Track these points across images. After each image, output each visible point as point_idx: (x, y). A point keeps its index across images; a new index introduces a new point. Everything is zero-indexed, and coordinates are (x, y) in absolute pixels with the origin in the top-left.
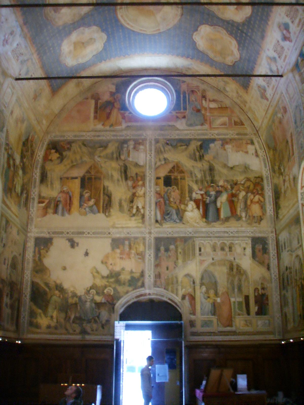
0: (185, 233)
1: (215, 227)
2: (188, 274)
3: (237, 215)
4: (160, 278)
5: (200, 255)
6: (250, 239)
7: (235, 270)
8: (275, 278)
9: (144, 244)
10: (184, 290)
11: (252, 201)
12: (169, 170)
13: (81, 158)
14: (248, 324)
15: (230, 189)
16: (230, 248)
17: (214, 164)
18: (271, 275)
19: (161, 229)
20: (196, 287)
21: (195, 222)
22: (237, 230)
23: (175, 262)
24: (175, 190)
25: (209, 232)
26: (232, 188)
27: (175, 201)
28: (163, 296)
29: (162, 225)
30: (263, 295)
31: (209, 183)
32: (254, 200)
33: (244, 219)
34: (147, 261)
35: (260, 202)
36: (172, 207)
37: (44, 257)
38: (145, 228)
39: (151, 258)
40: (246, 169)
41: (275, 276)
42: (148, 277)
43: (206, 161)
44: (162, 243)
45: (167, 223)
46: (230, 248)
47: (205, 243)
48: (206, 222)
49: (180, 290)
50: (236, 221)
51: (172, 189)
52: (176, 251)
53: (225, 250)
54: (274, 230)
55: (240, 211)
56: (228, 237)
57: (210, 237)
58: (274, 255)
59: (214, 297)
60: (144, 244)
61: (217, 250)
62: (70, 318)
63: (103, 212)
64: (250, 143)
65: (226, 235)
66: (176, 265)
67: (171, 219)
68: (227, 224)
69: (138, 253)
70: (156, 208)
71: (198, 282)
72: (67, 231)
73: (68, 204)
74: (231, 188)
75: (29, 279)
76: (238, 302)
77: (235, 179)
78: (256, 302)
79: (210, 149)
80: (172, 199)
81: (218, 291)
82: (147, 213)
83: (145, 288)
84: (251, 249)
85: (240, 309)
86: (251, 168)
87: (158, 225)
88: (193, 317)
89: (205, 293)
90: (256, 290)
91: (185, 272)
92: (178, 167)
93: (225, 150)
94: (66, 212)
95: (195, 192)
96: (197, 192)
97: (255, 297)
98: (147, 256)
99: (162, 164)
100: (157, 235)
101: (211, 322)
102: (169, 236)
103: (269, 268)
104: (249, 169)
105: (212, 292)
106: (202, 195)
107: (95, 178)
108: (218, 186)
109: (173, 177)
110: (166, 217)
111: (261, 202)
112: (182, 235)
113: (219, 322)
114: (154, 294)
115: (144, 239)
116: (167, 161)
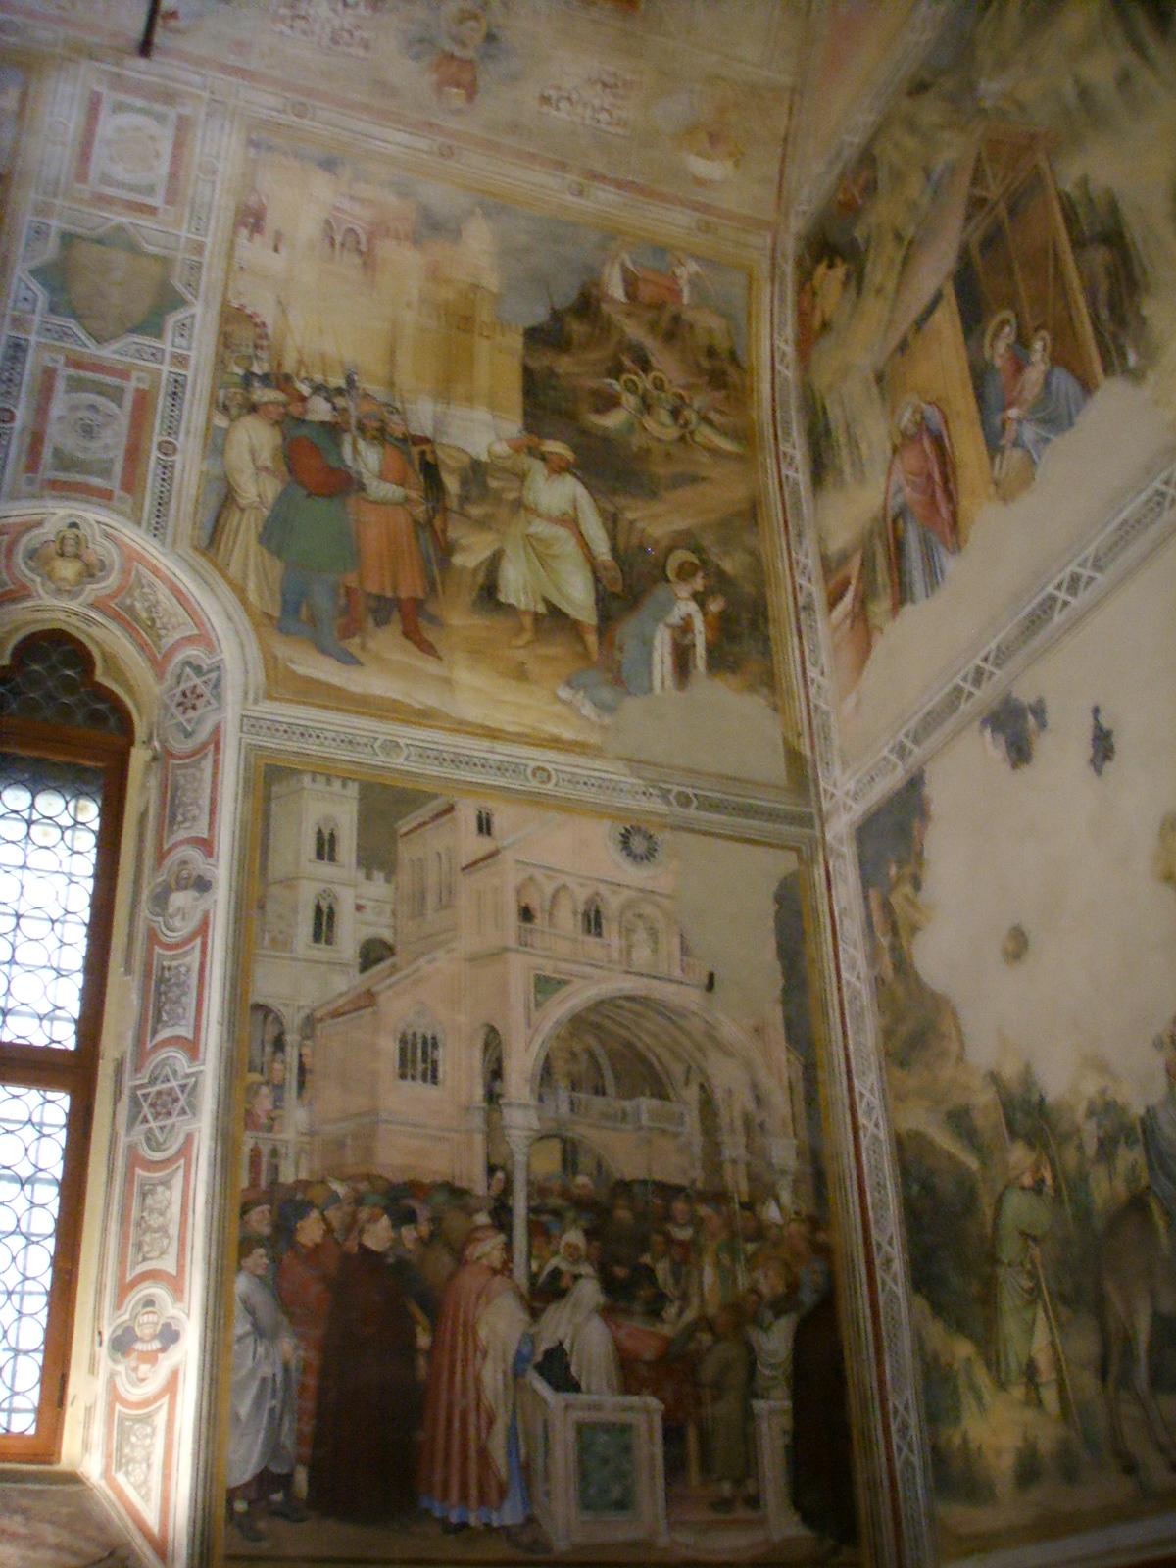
13: (927, 173)
37: (914, 929)
62: (1128, 1341)
63: (1108, 370)
72: (970, 668)
73: (939, 494)
75: (882, 1134)
94: (942, 549)
107: (1013, 211)
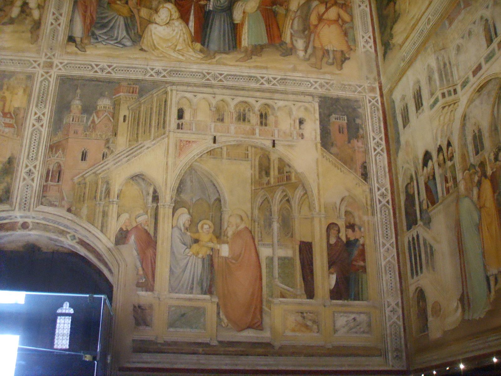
0: (146, 72)
1: (225, 64)
2: (142, 175)
3: (283, 43)
4: (58, 182)
5: (179, 127)
6: (317, 100)
7: (274, 173)
8: (384, 202)
9: (28, 92)
10: (125, 217)
11: (320, 19)
14: (309, 323)
16: (263, 117)
18: (371, 190)
19: (81, 59)
20: (161, 211)
21: (174, 50)
22: (283, 77)
23: (108, 141)
25: (208, 73)
28: (62, 233)
29: (84, 48)
30: (350, 244)
32: (325, 17)
34: (28, 131)
35: (340, 21)
38: (38, 52)
39: (42, 126)
41: (383, 195)
42: (23, 175)
44: (79, 91)
46: (263, 117)
47: (195, 100)
48: (201, 51)
49: (115, 215)
50: (281, 55)
52: (114, 115)
53: (249, 121)
54: (377, 85)
56: (259, 90)
57: (211, 86)
58: (378, 144)
59: (211, 240)
60: (28, 92)
61: (226, 119)
65: (253, 85)
66: (108, 148)
67: (111, 38)
68: (257, 61)
69: (6, 110)
70: (73, 11)
71: (167, 197)
76: (280, 258)
78: (331, 264)
81: (225, 225)
82: (49, 19)
83: (11, 205)
84: (318, 122)
85: (286, 277)
87: (72, 48)
88: (144, 297)
89: (187, 229)
90: (330, 227)
91: (135, 167)
97: (329, 245)
98: (31, 120)
100: (64, 72)
101: (199, 312)
102: (100, 75)
103: (365, 176)
105: (206, 227)
110: (98, 32)
111: (344, 22)
112: (133, 77)
113: (222, 316)
114: (37, 226)
115: (30, 77)
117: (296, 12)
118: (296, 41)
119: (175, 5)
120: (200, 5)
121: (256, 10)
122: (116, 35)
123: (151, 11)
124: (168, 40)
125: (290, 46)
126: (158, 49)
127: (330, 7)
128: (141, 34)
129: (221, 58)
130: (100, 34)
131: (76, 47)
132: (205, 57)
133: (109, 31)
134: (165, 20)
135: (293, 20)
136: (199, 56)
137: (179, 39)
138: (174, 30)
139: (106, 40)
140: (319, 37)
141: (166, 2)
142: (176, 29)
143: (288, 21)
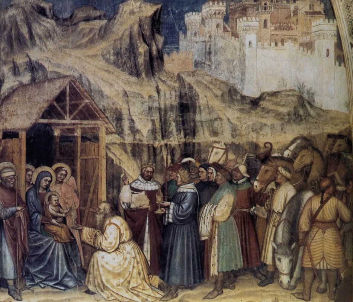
11: (313, 220)
12: (46, 105)
15: (244, 177)
17: (198, 89)
24: (66, 175)
26: (253, 172)
27: (64, 215)
31: (177, 156)
32: (318, 218)
33: (285, 279)
36: (55, 234)
40: (303, 106)
43: (169, 75)
45: (37, 289)
48: (160, 287)
51: (53, 175)
55: (274, 252)
64: (322, 12)
74: (248, 172)
77: (262, 139)
79: (185, 33)
80: (52, 209)
86: (318, 101)
92: (75, 94)
93: (235, 35)
95: (130, 184)
96: (133, 185)
99: (22, 86)
104: (312, 106)
106: (151, 195)
108: (206, 166)
109: (57, 133)
116: (39, 75)
117: (281, 214)
118: (280, 260)
119: (126, 219)
120: (156, 216)
121: (229, 217)
122: (55, 273)
123: (96, 231)
124: (119, 275)
125: (271, 269)
126: (108, 289)
127: (328, 199)
128: (85, 268)
129: (185, 295)
130: (36, 272)
131: (9, 293)
132: (163, 297)
133: (46, 266)
134: (113, 244)
135: (277, 227)
136: (158, 296)
137: (133, 271)
138: (126, 259)
139: (44, 280)
140: (309, 251)
141: (113, 216)
142: (128, 256)
143: (270, 230)
